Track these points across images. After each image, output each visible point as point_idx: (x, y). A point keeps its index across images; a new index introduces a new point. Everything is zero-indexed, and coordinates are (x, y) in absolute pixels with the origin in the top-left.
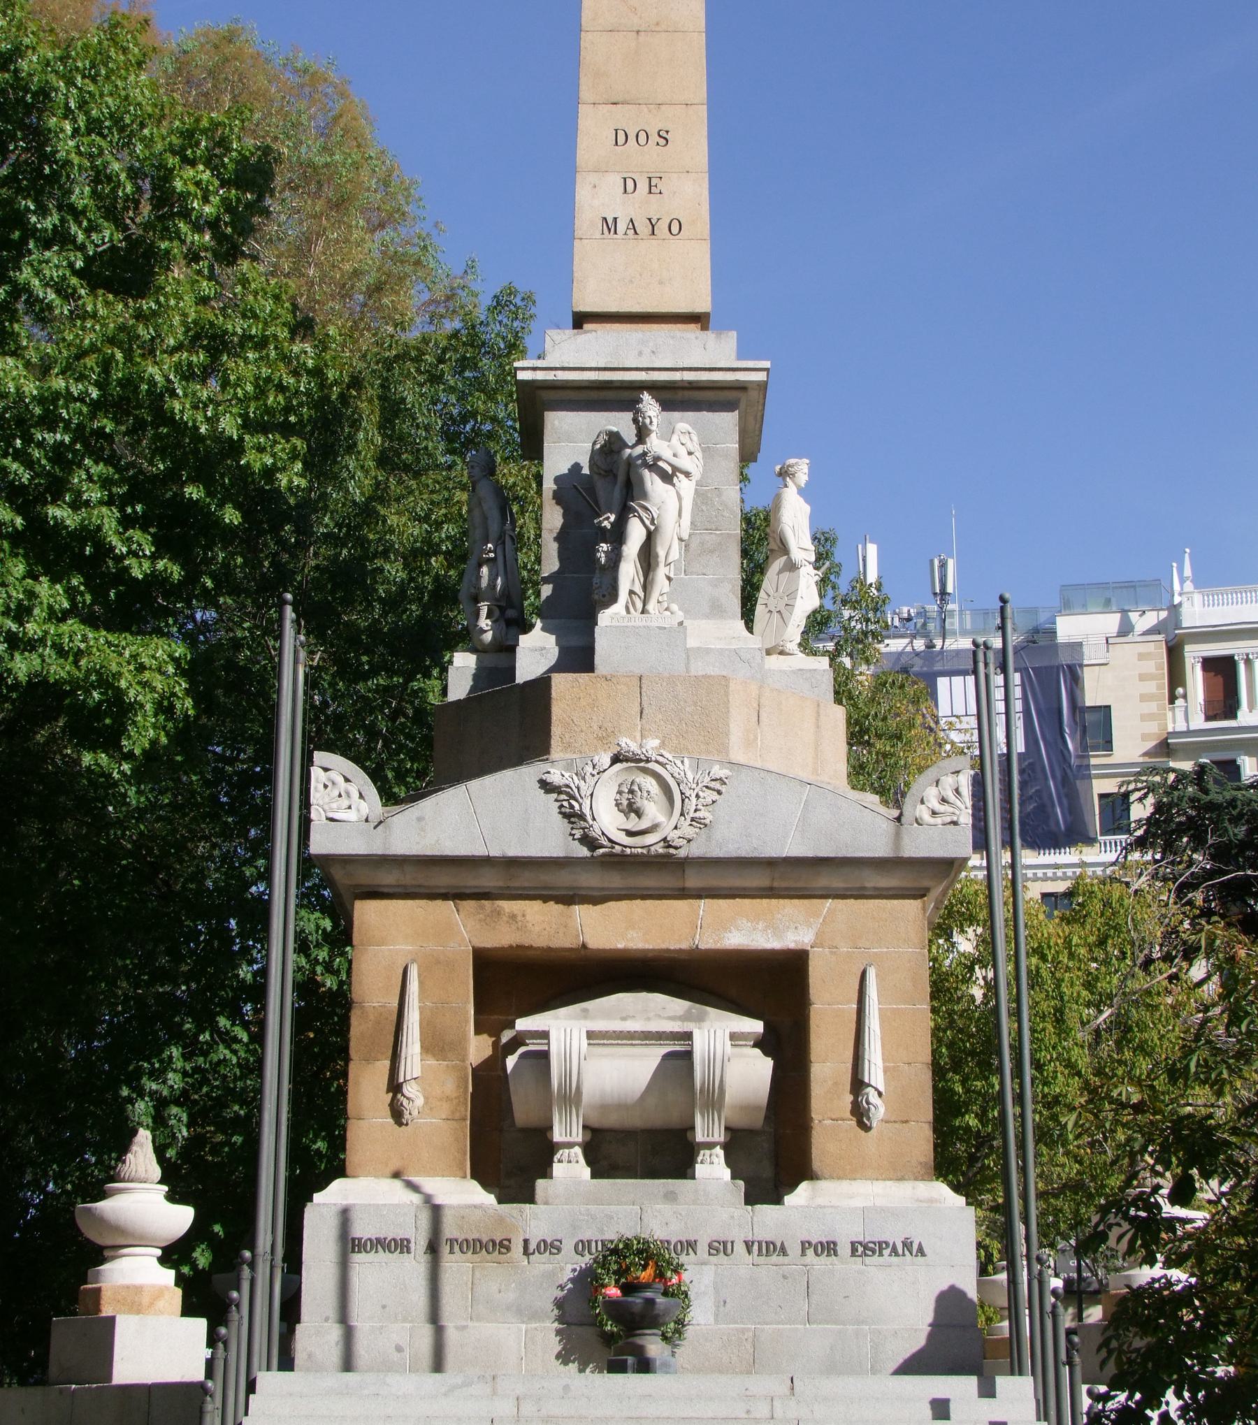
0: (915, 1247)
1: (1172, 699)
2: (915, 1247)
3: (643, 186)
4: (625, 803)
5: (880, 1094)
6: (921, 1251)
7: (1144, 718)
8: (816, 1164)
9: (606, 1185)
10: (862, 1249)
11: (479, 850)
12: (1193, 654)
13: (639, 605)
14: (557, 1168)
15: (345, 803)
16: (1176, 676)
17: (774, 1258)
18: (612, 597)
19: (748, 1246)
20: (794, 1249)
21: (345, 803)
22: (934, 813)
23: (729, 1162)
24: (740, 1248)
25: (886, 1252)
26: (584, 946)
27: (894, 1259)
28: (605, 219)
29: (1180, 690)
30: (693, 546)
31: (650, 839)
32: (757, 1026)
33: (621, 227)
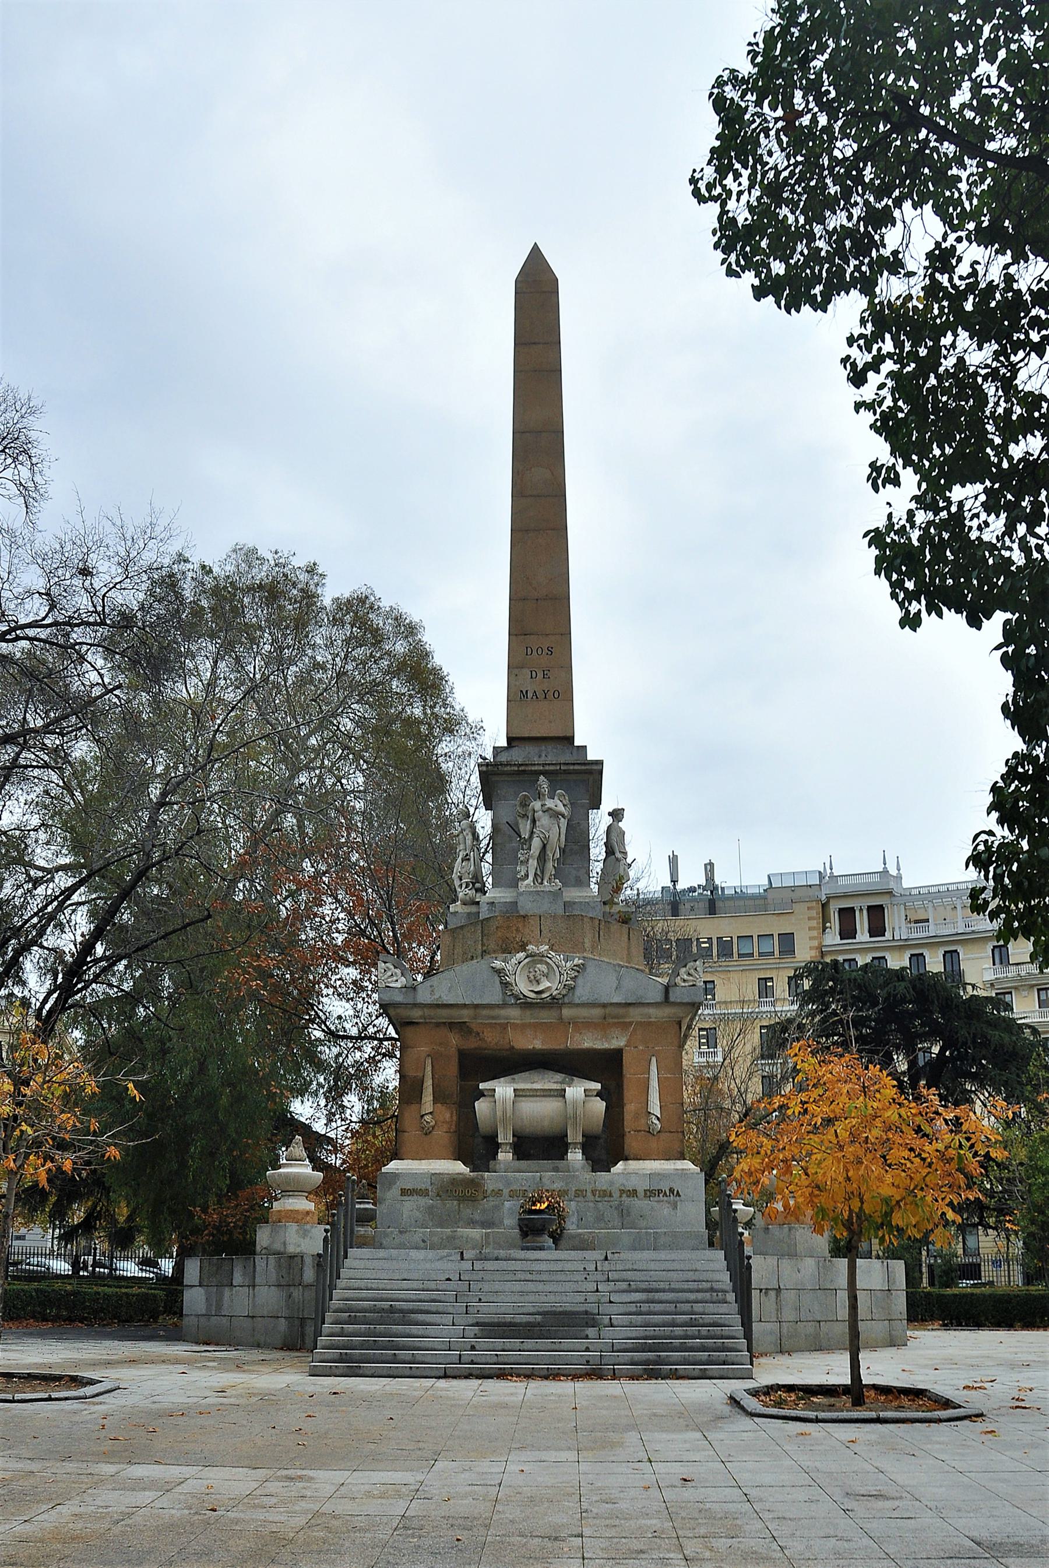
0: (675, 1192)
1: (824, 929)
2: (675, 1192)
3: (540, 675)
4: (532, 978)
5: (658, 1119)
6: (678, 1194)
7: (811, 938)
8: (626, 1153)
9: (523, 1164)
10: (650, 1193)
11: (461, 1001)
12: (834, 907)
13: (540, 881)
14: (501, 1156)
15: (395, 978)
16: (825, 919)
17: (606, 1199)
18: (527, 876)
19: (593, 1192)
20: (616, 1195)
21: (395, 978)
22: (684, 981)
23: (583, 1154)
24: (589, 1194)
25: (661, 1195)
26: (513, 1047)
27: (665, 1198)
28: (521, 691)
29: (828, 925)
30: (567, 850)
31: (544, 996)
32: (598, 1086)
33: (530, 695)
